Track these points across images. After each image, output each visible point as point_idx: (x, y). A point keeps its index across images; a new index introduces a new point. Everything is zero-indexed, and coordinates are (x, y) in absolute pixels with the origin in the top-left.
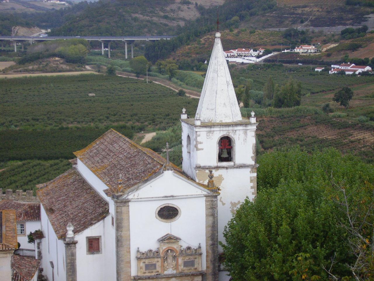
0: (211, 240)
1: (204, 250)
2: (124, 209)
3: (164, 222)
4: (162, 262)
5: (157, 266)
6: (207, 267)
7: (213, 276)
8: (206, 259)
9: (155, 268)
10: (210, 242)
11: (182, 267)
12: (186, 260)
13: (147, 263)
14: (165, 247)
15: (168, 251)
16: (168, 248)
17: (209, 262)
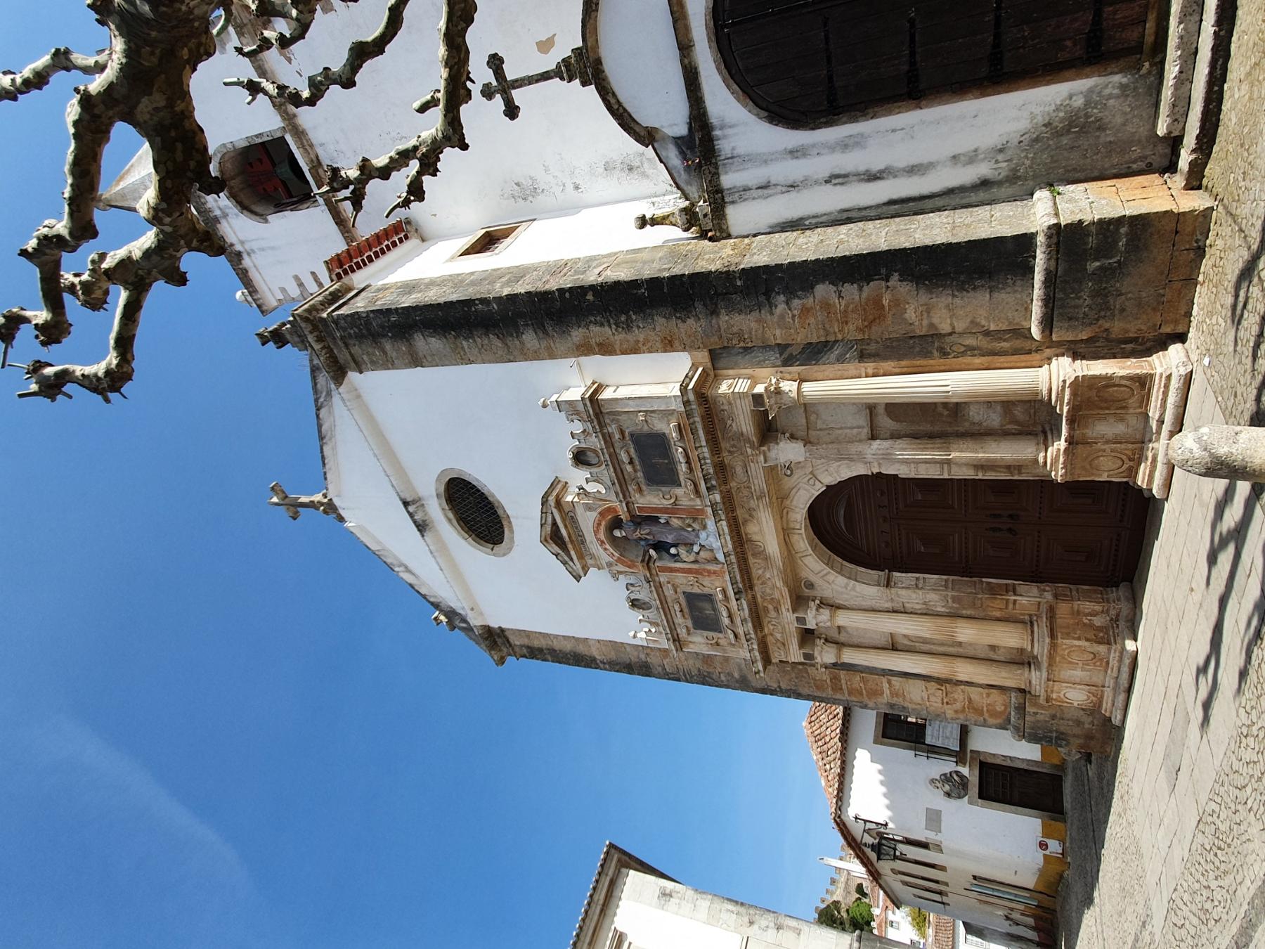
0: (519, 334)
1: (570, 378)
2: (516, 641)
3: (512, 531)
4: (671, 570)
5: (696, 590)
6: (669, 345)
7: (721, 304)
8: (624, 352)
9: (709, 598)
10: (529, 338)
11: (679, 491)
12: (640, 474)
13: (689, 623)
14: (601, 552)
15: (614, 541)
16: (602, 542)
17: (639, 335)
